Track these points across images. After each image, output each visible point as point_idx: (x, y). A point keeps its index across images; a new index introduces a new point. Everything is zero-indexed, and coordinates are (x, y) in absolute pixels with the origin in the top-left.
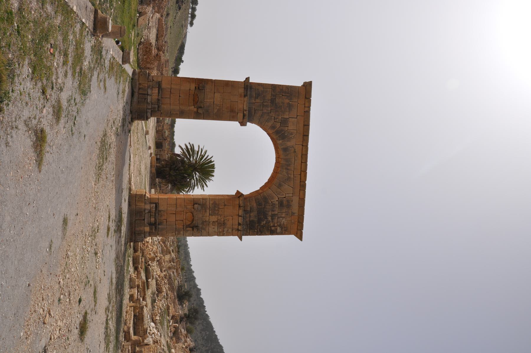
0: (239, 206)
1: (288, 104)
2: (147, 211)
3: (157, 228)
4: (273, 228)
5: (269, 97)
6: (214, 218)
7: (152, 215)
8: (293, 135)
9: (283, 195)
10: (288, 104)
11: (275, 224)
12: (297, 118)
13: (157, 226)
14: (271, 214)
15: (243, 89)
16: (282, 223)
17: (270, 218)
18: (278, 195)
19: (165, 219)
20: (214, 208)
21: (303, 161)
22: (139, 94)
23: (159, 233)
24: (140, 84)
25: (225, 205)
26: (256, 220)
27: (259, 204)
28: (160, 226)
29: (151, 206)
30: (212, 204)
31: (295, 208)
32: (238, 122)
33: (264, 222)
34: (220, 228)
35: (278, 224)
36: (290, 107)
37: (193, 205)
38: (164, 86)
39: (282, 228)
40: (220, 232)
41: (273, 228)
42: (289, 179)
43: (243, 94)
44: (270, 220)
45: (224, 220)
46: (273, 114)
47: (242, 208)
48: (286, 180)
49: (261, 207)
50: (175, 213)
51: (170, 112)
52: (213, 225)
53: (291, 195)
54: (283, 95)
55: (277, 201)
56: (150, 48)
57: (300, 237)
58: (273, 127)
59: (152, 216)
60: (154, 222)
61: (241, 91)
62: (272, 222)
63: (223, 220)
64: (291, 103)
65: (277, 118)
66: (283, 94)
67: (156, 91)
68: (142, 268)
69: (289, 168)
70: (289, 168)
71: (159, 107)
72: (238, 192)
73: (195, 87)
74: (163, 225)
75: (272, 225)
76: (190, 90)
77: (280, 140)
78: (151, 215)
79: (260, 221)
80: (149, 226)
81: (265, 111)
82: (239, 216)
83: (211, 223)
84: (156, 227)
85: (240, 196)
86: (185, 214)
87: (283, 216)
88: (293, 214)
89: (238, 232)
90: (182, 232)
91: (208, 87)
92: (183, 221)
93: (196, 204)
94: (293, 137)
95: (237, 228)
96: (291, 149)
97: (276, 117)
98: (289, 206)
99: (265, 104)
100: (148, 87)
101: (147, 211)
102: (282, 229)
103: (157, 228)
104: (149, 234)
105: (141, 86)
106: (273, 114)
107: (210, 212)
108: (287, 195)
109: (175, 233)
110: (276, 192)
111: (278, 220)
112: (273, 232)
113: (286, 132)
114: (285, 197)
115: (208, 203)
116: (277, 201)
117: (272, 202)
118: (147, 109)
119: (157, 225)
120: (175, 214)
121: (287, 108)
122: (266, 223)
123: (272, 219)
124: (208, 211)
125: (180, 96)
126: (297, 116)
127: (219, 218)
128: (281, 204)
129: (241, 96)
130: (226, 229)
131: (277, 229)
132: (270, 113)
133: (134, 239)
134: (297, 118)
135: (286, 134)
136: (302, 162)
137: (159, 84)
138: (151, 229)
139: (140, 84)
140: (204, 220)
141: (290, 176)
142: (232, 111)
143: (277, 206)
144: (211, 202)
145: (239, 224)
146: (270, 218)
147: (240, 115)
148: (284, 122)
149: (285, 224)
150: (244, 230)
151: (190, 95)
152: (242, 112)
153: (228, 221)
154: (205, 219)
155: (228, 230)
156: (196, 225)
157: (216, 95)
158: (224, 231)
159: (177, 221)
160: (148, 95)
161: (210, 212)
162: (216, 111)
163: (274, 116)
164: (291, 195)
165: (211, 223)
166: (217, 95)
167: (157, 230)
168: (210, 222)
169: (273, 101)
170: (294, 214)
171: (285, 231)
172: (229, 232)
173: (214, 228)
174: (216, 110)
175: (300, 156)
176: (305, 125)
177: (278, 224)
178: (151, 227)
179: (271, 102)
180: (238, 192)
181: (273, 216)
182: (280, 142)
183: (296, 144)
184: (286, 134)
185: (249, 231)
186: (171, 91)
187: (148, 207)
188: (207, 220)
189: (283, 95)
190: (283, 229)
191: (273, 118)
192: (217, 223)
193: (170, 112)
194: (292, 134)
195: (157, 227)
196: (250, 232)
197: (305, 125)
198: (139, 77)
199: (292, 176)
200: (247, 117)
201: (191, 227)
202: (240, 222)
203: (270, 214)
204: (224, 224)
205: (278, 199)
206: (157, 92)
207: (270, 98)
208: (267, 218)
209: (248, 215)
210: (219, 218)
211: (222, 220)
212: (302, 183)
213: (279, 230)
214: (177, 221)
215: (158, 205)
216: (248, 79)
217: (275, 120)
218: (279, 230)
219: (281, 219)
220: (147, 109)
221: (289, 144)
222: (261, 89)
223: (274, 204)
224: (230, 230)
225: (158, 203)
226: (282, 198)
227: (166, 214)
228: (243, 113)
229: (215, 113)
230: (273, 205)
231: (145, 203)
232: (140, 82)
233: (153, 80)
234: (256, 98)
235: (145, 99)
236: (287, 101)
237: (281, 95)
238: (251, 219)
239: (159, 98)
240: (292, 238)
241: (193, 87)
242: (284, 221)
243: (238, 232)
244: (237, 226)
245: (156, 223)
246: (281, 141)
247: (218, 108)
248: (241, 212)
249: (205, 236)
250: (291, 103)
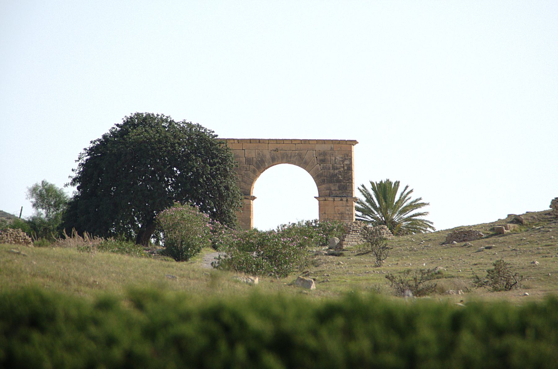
4: (346, 168)
8: (260, 153)
9: (314, 160)
11: (341, 166)
12: (245, 150)
14: (332, 171)
17: (336, 171)
18: (315, 164)
21: (283, 143)
25: (325, 213)
27: (324, 181)
31: (327, 147)
33: (340, 176)
35: (341, 163)
39: (345, 159)
40: (349, 217)
41: (346, 168)
44: (338, 171)
45: (339, 214)
46: (243, 172)
47: (326, 198)
48: (300, 158)
49: (326, 180)
55: (320, 165)
57: (355, 142)
58: (254, 172)
62: (339, 169)
65: (246, 169)
69: (289, 155)
70: (289, 155)
77: (265, 165)
79: (339, 181)
82: (334, 200)
88: (332, 149)
97: (245, 169)
98: (324, 154)
102: (347, 159)
106: (243, 172)
108: (314, 156)
110: (312, 166)
111: (338, 163)
112: (350, 168)
114: (317, 157)
116: (320, 165)
121: (237, 159)
122: (340, 175)
123: (337, 169)
126: (243, 150)
128: (323, 161)
130: (347, 212)
131: (347, 164)
134: (245, 150)
135: (260, 159)
141: (296, 154)
143: (325, 164)
145: (341, 200)
146: (336, 171)
148: (249, 161)
149: (341, 156)
153: (339, 210)
158: (348, 214)
163: (244, 171)
170: (332, 148)
171: (348, 157)
175: (278, 145)
177: (341, 163)
181: (334, 168)
184: (260, 159)
185: (348, 191)
190: (347, 158)
191: (246, 172)
194: (259, 154)
202: (339, 200)
203: (332, 171)
204: (342, 213)
208: (336, 174)
209: (334, 192)
211: (338, 215)
212: (303, 142)
213: (347, 162)
217: (248, 170)
218: (347, 162)
219: (336, 160)
221: (268, 156)
223: (323, 167)
224: (348, 208)
230: (324, 168)
238: (337, 189)
240: (355, 148)
244: (343, 202)
246: (266, 164)
247: (241, 222)
248: (331, 199)
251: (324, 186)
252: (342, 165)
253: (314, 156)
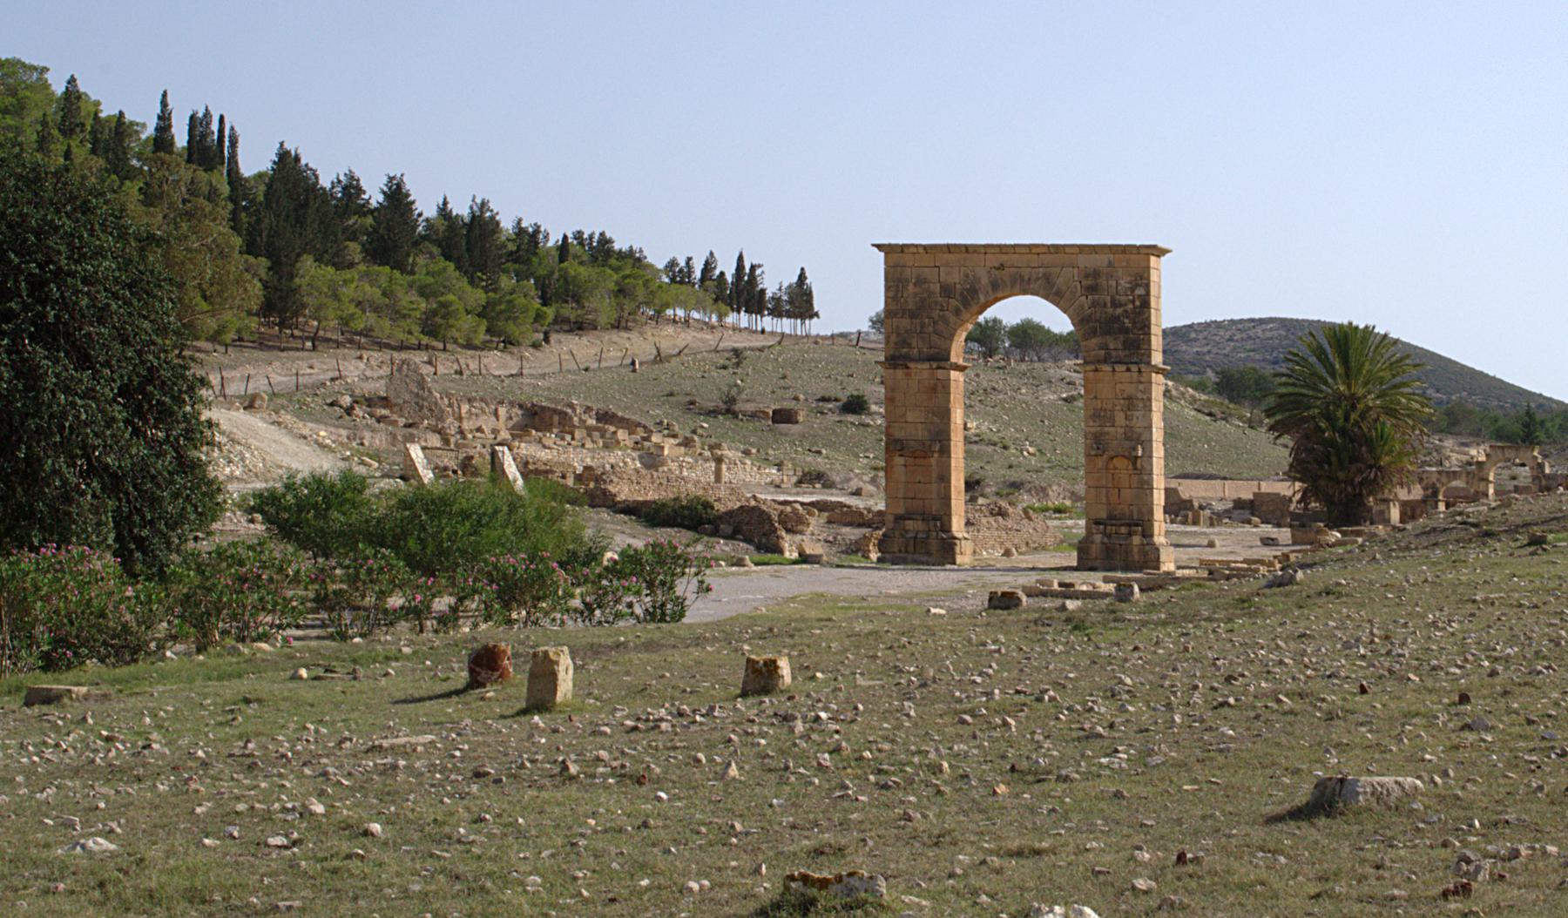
0: (1097, 370)
2: (1106, 540)
4: (1138, 303)
5: (905, 323)
6: (1120, 418)
10: (915, 284)
22: (915, 552)
24: (900, 551)
26: (1122, 338)
31: (1100, 261)
33: (1126, 321)
36: (920, 281)
38: (901, 511)
39: (1138, 285)
40: (1145, 406)
41: (1138, 303)
42: (1047, 277)
46: (936, 313)
53: (1076, 270)
61: (900, 373)
67: (910, 524)
69: (1026, 278)
70: (1026, 278)
75: (1131, 306)
81: (931, 329)
87: (1114, 283)
88: (1110, 264)
90: (1145, 477)
91: (899, 434)
98: (1096, 274)
99: (918, 329)
100: (902, 536)
115: (1093, 430)
123: (1120, 305)
127: (1118, 408)
128: (1092, 289)
129: (908, 375)
130: (1140, 395)
137: (899, 518)
139: (900, 551)
144: (1091, 423)
145: (1128, 370)
146: (1119, 311)
147: (940, 374)
148: (947, 291)
157: (909, 420)
160: (915, 538)
164: (1076, 270)
166: (910, 417)
169: (913, 315)
171: (1142, 280)
175: (1005, 257)
181: (1115, 304)
182: (982, 299)
187: (1098, 538)
194: (967, 276)
200: (942, 364)
203: (1110, 310)
204: (1129, 398)
207: (908, 321)
209: (1114, 354)
210: (1118, 408)
213: (1140, 291)
218: (1140, 291)
221: (985, 281)
224: (1141, 387)
230: (1094, 304)
232: (896, 549)
234: (909, 345)
236: (911, 287)
238: (1120, 346)
241: (899, 460)
242: (1124, 283)
248: (1107, 368)
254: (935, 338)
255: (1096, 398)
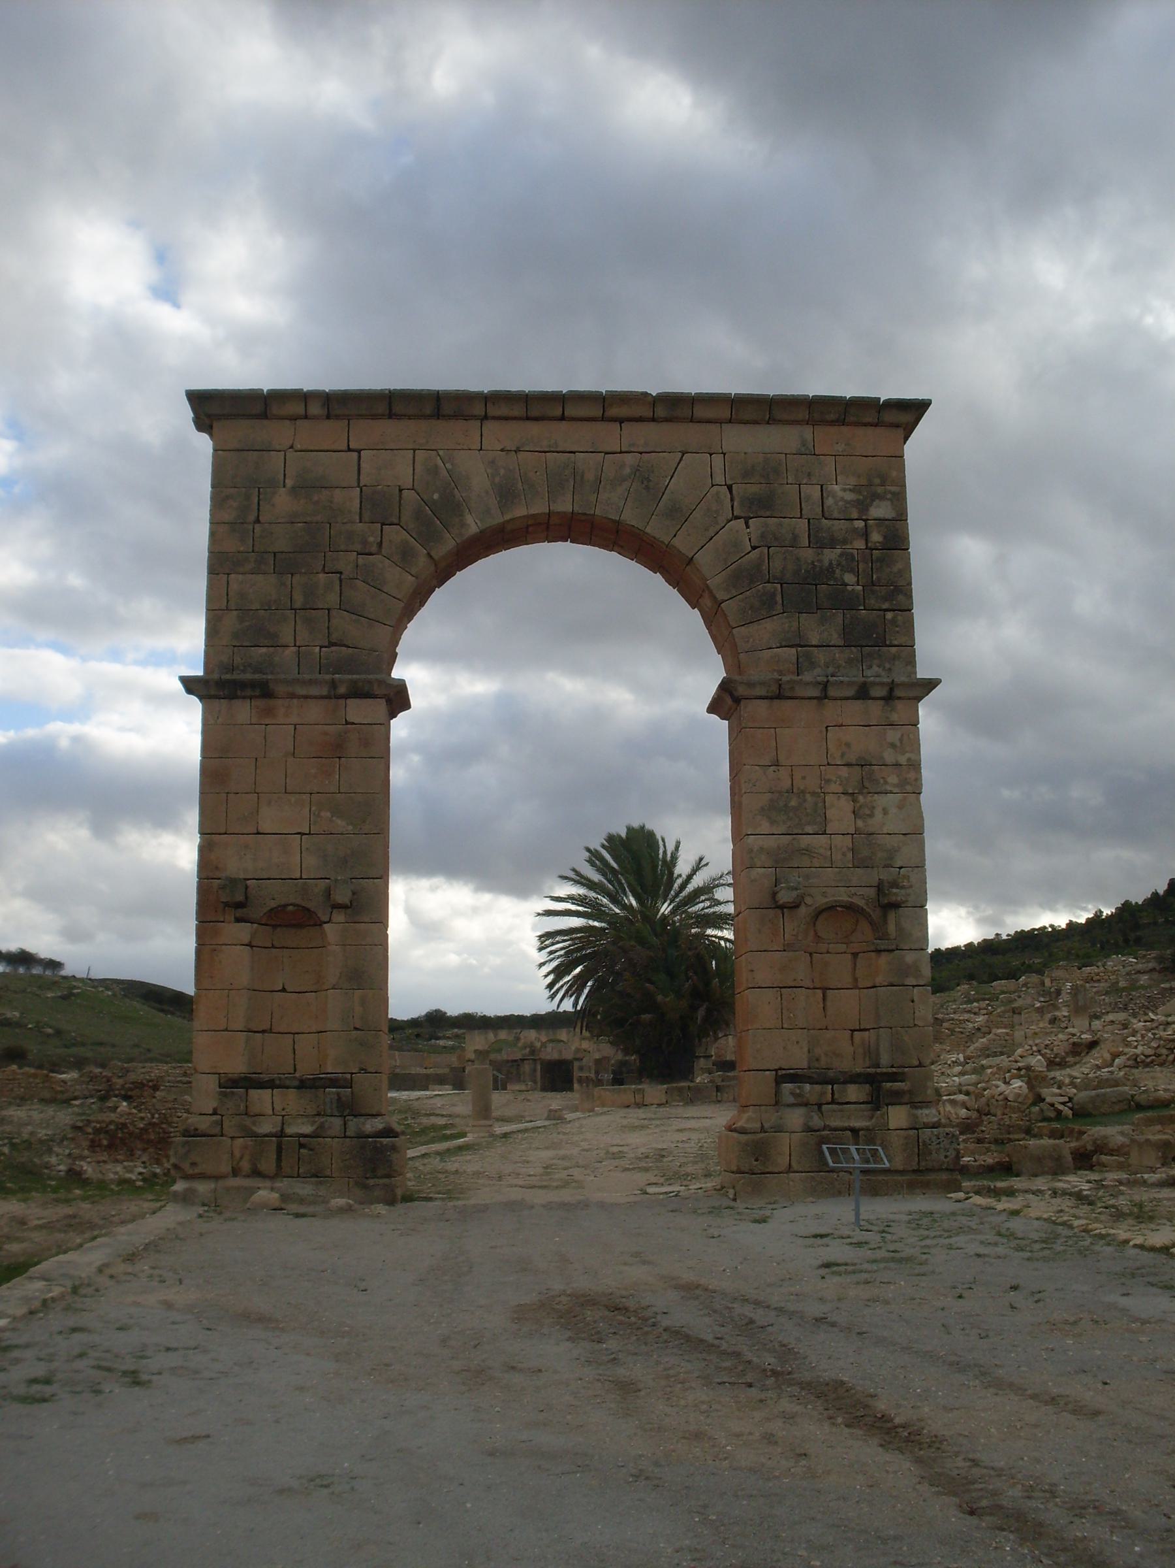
1: (294, 492)
3: (894, 1070)
4: (876, 537)
5: (263, 586)
6: (840, 813)
7: (833, 1094)
8: (436, 466)
11: (855, 530)
12: (359, 451)
13: (884, 1070)
14: (810, 551)
15: (237, 703)
16: (849, 496)
17: (831, 555)
18: (722, 520)
19: (852, 1036)
20: (791, 814)
23: (916, 1063)
25: (776, 764)
27: (765, 607)
28: (885, 1059)
29: (791, 1100)
30: (773, 822)
32: (392, 722)
33: (849, 578)
34: (886, 783)
35: (855, 515)
37: (779, 911)
39: (875, 497)
40: (903, 783)
41: (876, 537)
43: (261, 703)
44: (839, 551)
45: (848, 765)
48: (647, 488)
49: (779, 598)
50: (819, 992)
51: (356, 1029)
52: (871, 816)
54: (258, 521)
55: (748, 527)
56: (97, 1131)
59: (836, 1096)
60: (867, 1086)
61: (244, 711)
62: (845, 542)
63: (845, 768)
64: (289, 483)
65: (365, 542)
66: (252, 517)
67: (261, 1099)
68: (1082, 1133)
69: (590, 476)
70: (590, 476)
71: (334, 1083)
72: (714, 708)
73: (238, 920)
74: (878, 1049)
75: (860, 544)
76: (250, 945)
77: (463, 525)
78: (833, 1102)
79: (844, 602)
80: (884, 1110)
81: (333, 599)
83: (860, 823)
84: (885, 1074)
85: (731, 695)
86: (823, 947)
89: (899, 698)
92: (855, 955)
93: (774, 894)
94: (448, 465)
95: (882, 702)
96: (502, 472)
97: (358, 547)
99: (299, 601)
101: (817, 1122)
102: (881, 498)
103: (894, 1070)
104: (921, 1108)
105: (246, 1165)
106: (346, 562)
107: (809, 829)
108: (719, 479)
109: (914, 986)
110: (707, 530)
111: (836, 515)
113: (425, 498)
114: (730, 488)
116: (748, 527)
117: (754, 548)
118: (348, 1134)
119: (879, 1070)
120: (825, 990)
121: (316, 498)
122: (851, 571)
123: (832, 543)
124: (805, 841)
125: (284, 990)
126: (349, 450)
127: (835, 787)
130: (889, 756)
132: (341, 573)
133: (944, 1176)
134: (359, 451)
135: (436, 496)
136: (562, 418)
138: (896, 1098)
139: (235, 1172)
140: (850, 855)
141: (627, 471)
142: (336, 749)
144: (765, 827)
146: (831, 555)
147: (358, 711)
149: (853, 481)
150: (890, 669)
151: (276, 944)
152: (342, 701)
153: (848, 745)
154: (844, 854)
155: (893, 746)
156: (872, 892)
157: (266, 827)
158: (897, 765)
159: (856, 980)
160: (281, 1134)
161: (809, 829)
162: (340, 824)
165: (860, 823)
167: (900, 1070)
168: (858, 831)
172: (901, 740)
173: (885, 812)
174: (339, 822)
176: (390, 410)
178: (887, 1101)
179: (292, 575)
180: (714, 708)
181: (819, 541)
183: (481, 449)
184: (436, 496)
185: (894, 649)
186: (263, 1032)
188: (848, 840)
189: (258, 521)
190: (880, 490)
191: (362, 560)
192: (861, 798)
193: (356, 1029)
194: (435, 471)
195: (890, 1070)
196: (896, 643)
197: (390, 410)
198: (203, 1176)
199: (629, 459)
201: (885, 917)
203: (808, 554)
205: (738, 518)
206: (266, 1094)
208: (830, 569)
210: (835, 787)
211: (844, 772)
213: (880, 510)
214: (856, 980)
215: (784, 1072)
216: (190, 685)
217: (374, 549)
218: (880, 510)
219: (829, 502)
220: (348, 1134)
222: (230, 621)
223: (763, 536)
224: (893, 735)
225: (776, 1070)
226: (732, 500)
227: (829, 1034)
228: (345, 697)
229: (350, 828)
230: (767, 541)
231: (779, 1129)
232: (225, 1168)
233: (215, 1113)
235: (302, 1146)
237: (258, 527)
238: (836, 639)
239: (296, 1083)
242: (840, 491)
243: (899, 698)
245: (869, 1074)
246: (469, 519)
249: (923, 850)
250: (289, 483)
251: (768, 629)
252: (860, 524)
253: (719, 479)
254: (343, 623)
255: (776, 764)
